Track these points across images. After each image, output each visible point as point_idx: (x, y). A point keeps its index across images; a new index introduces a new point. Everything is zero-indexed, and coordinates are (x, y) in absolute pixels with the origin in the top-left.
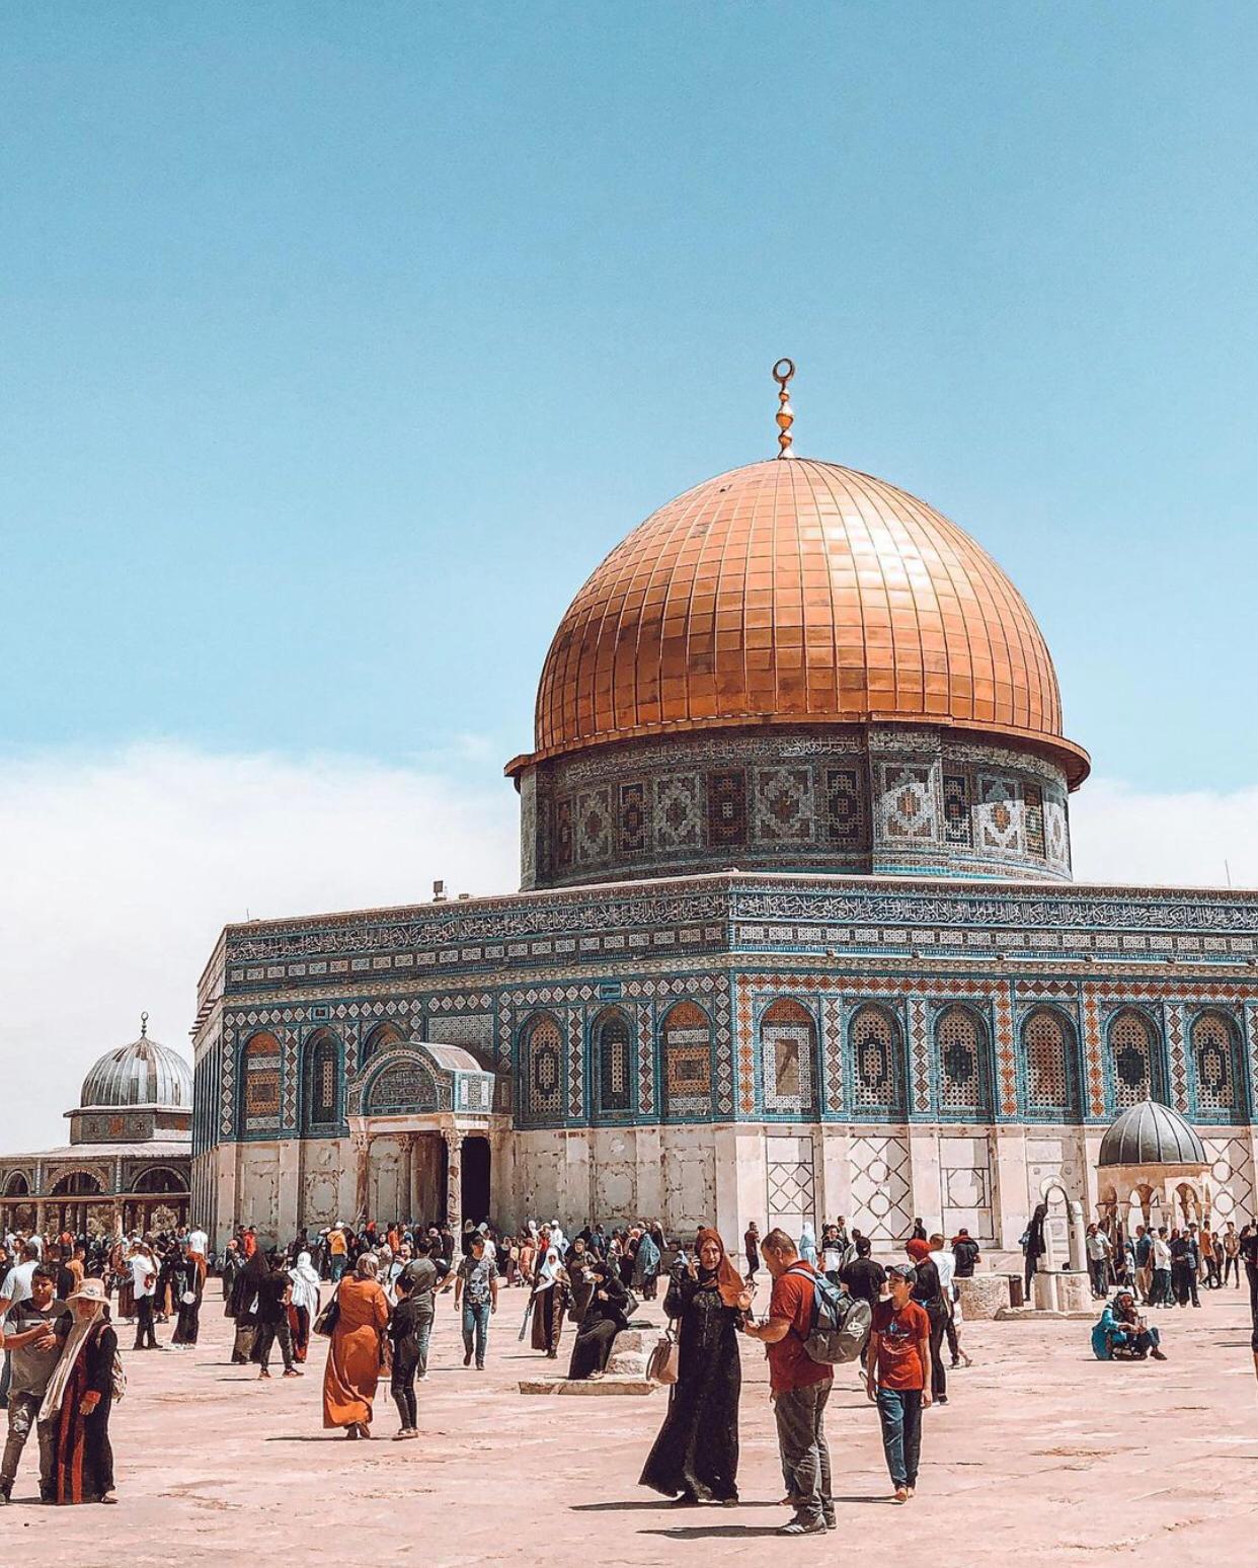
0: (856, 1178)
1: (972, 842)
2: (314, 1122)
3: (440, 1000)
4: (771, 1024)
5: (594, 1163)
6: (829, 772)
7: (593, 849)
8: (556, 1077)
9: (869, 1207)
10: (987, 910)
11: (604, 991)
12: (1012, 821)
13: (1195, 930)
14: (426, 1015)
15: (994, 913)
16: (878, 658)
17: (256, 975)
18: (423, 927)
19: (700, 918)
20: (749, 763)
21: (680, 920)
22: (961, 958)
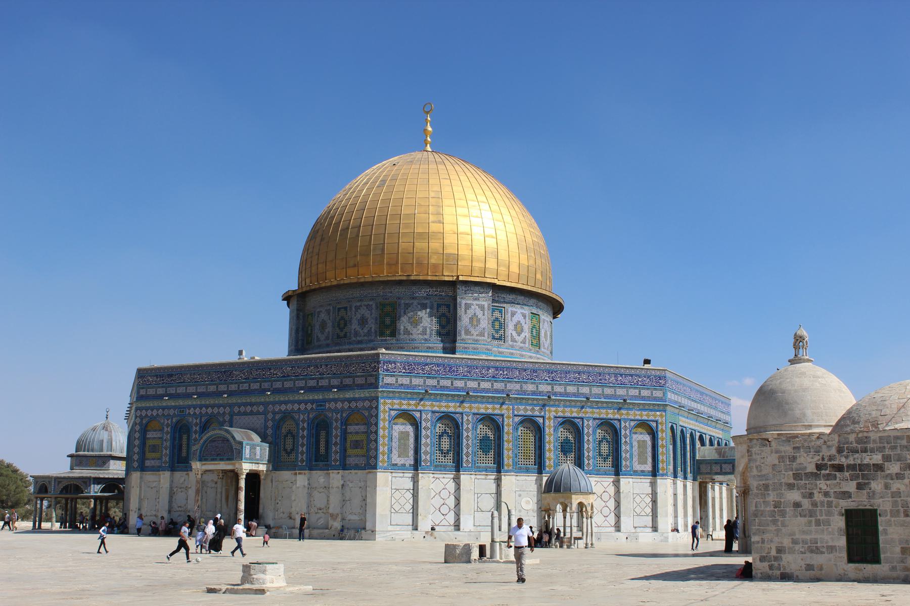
0: (434, 497)
1: (504, 340)
2: (177, 463)
3: (239, 407)
4: (396, 424)
5: (310, 488)
6: (437, 304)
7: (322, 337)
9: (440, 511)
11: (318, 406)
12: (524, 331)
13: (600, 384)
14: (232, 415)
15: (507, 374)
16: (463, 252)
17: (151, 392)
18: (232, 372)
20: (399, 299)
22: (490, 395)
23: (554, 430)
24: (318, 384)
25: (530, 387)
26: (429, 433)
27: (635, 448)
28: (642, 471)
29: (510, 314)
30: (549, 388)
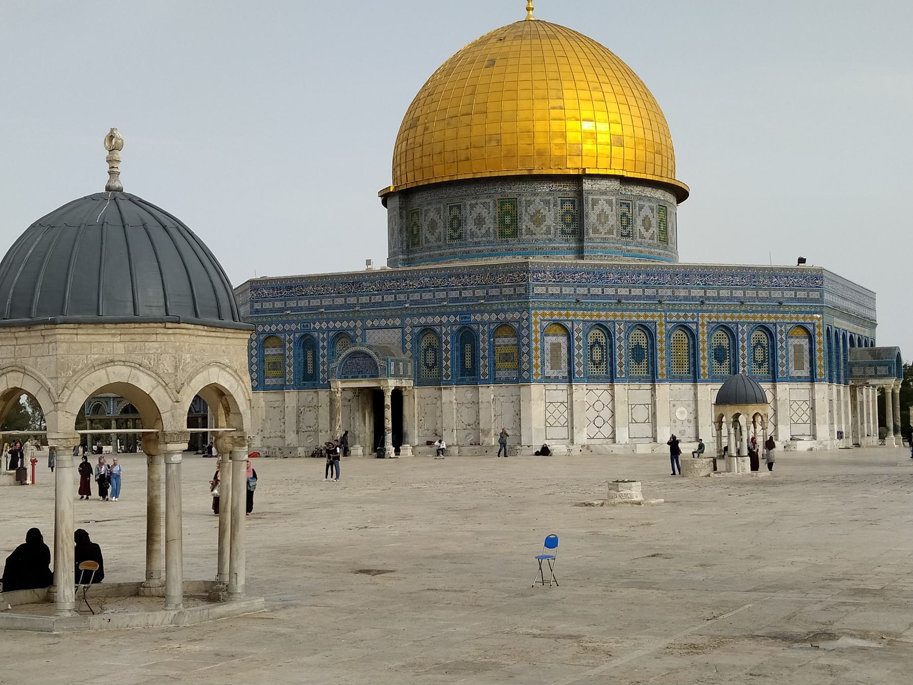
2: (304, 380)
4: (547, 335)
6: (561, 200)
7: (432, 239)
8: (436, 361)
9: (594, 423)
10: (655, 278)
12: (652, 225)
15: (658, 279)
17: (267, 305)
18: (362, 283)
19: (513, 282)
20: (520, 195)
21: (503, 283)
23: (708, 336)
24: (460, 295)
25: (682, 293)
26: (581, 343)
27: (791, 353)
28: (799, 377)
29: (637, 208)
30: (702, 293)
